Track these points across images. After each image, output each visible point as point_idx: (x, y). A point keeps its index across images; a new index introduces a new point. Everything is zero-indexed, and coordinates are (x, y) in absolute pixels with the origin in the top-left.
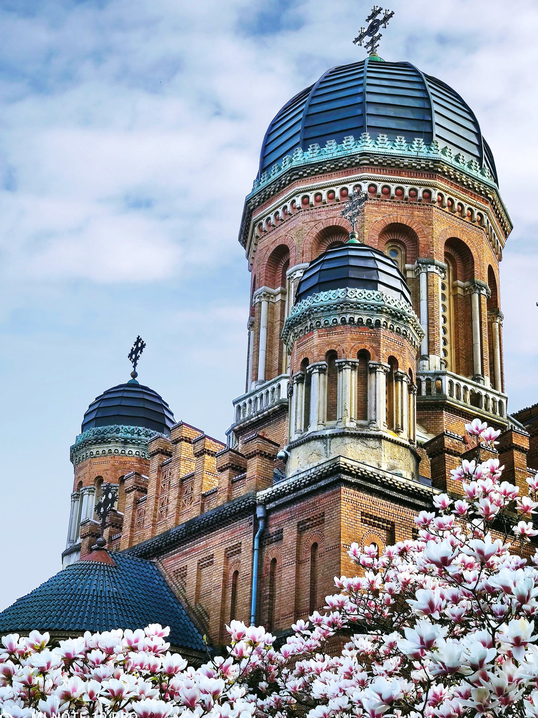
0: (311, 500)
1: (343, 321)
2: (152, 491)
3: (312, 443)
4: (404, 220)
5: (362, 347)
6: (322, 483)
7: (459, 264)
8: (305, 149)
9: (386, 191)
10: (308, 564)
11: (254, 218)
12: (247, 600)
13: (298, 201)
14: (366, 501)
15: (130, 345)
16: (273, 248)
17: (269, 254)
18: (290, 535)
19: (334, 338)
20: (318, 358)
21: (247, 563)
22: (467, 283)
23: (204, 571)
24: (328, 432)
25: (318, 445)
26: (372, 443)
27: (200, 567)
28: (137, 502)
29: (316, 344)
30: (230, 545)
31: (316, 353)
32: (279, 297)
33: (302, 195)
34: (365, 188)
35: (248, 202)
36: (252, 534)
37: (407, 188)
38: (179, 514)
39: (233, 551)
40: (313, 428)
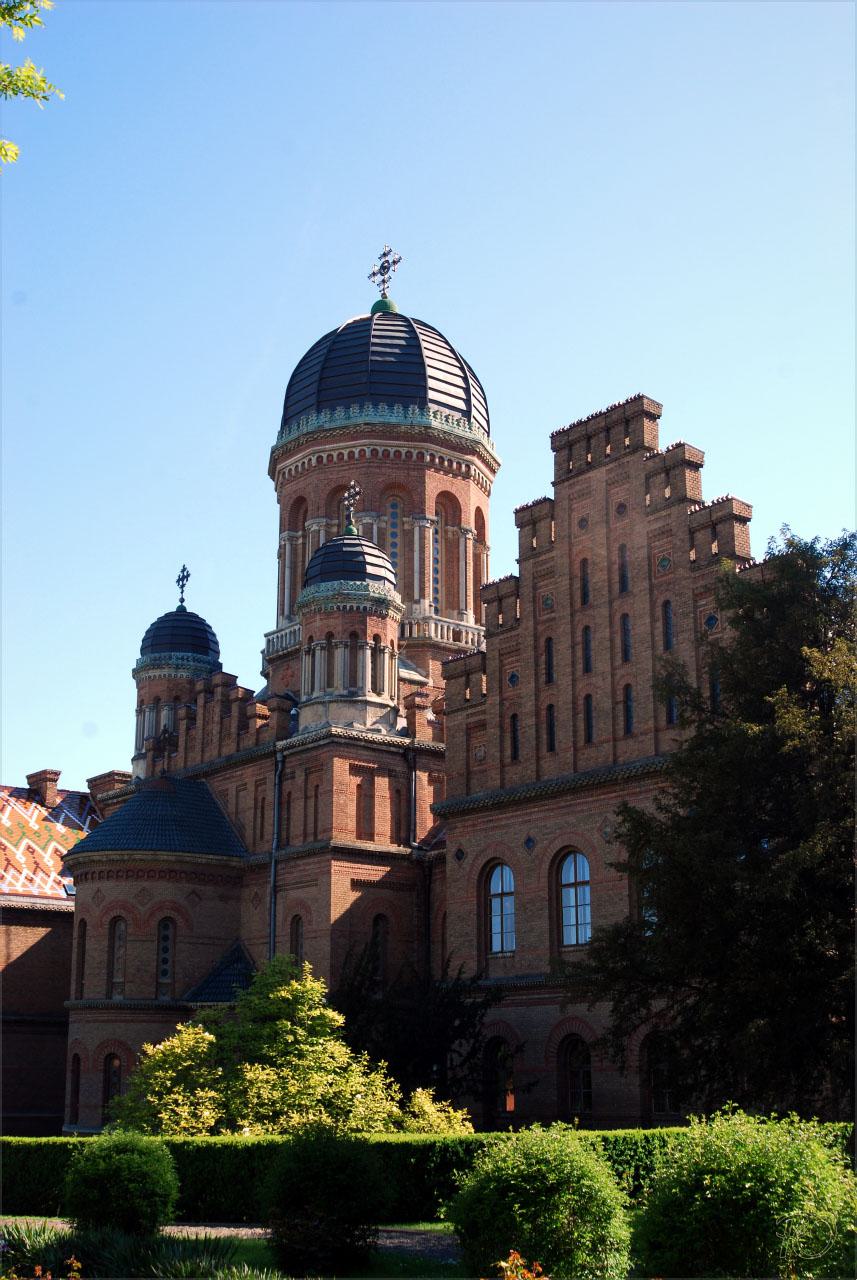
0: (314, 753)
1: (338, 608)
2: (199, 722)
3: (315, 706)
5: (352, 629)
6: (322, 743)
8: (319, 412)
10: (313, 800)
11: (279, 467)
12: (272, 822)
15: (178, 573)
17: (292, 501)
18: (300, 778)
19: (332, 622)
21: (271, 796)
22: (455, 528)
23: (241, 793)
25: (321, 708)
26: (359, 706)
27: (238, 792)
28: (188, 729)
30: (259, 778)
31: (318, 634)
32: (300, 541)
33: (317, 455)
34: (368, 454)
35: (273, 452)
36: (273, 772)
37: (403, 451)
38: (220, 747)
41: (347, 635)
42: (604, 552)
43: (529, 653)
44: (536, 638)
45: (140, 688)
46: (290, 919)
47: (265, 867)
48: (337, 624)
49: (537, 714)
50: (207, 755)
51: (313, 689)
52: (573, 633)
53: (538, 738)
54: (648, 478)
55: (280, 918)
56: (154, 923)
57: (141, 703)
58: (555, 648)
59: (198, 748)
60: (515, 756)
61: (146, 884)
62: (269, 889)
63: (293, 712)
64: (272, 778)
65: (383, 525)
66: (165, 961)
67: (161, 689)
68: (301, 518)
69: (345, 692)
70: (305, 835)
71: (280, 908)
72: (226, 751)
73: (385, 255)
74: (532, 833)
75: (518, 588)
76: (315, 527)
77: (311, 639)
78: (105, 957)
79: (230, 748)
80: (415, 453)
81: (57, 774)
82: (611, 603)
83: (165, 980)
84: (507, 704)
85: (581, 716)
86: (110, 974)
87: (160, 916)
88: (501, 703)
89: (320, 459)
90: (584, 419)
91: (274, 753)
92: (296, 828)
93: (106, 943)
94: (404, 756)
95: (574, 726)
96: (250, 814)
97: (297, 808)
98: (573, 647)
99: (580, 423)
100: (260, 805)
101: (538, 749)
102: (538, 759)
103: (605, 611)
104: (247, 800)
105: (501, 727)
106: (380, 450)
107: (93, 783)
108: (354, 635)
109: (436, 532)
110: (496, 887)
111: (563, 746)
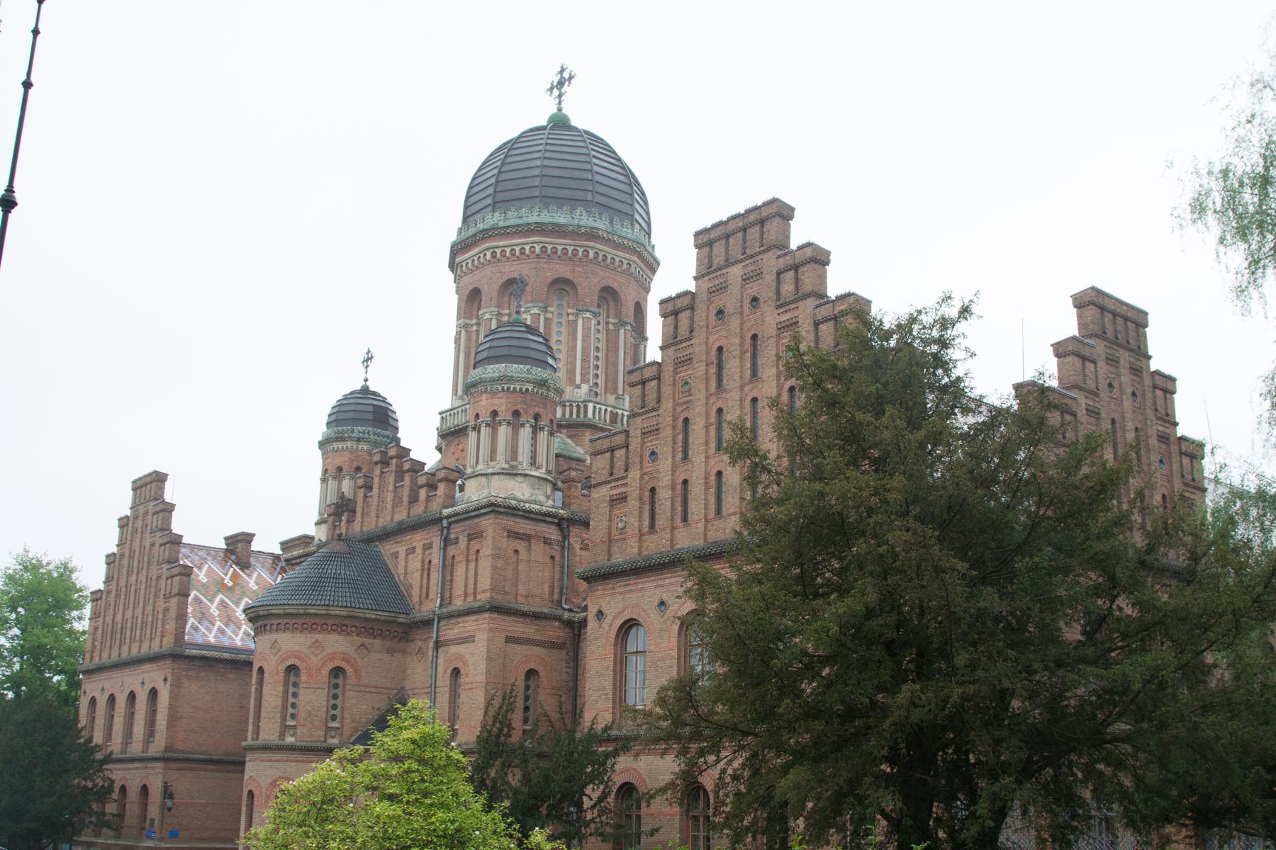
0: (476, 520)
2: (375, 490)
4: (568, 275)
7: (612, 304)
8: (494, 211)
9: (555, 252)
11: (458, 260)
13: (489, 256)
14: (510, 522)
15: (363, 355)
16: (470, 288)
18: (463, 542)
19: (497, 401)
20: (485, 417)
21: (436, 556)
24: (490, 471)
25: (483, 479)
28: (366, 497)
29: (485, 404)
32: (475, 328)
37: (570, 249)
38: (393, 512)
39: (428, 547)
40: (480, 467)
41: (510, 413)
42: (737, 341)
43: (667, 433)
44: (675, 419)
45: (324, 459)
46: (449, 671)
47: (428, 623)
48: (502, 404)
49: (673, 489)
50: (381, 520)
51: (477, 462)
52: (707, 414)
53: (673, 510)
54: (779, 274)
55: (440, 669)
56: (326, 672)
57: (325, 471)
58: (691, 427)
59: (373, 514)
60: (652, 525)
61: (319, 637)
62: (431, 645)
63: (459, 482)
64: (437, 542)
65: (550, 316)
66: (335, 707)
67: (342, 460)
68: (476, 307)
69: (506, 466)
70: (466, 595)
71: (441, 661)
72: (398, 517)
73: (562, 71)
74: (665, 598)
75: (660, 372)
76: (487, 316)
77: (477, 416)
78: (280, 702)
79: (401, 515)
80: (581, 250)
81: (253, 535)
82: (742, 387)
83: (335, 724)
84: (646, 478)
85: (713, 490)
86: (284, 719)
87: (331, 665)
88: (641, 478)
89: (494, 254)
90: (725, 219)
91: (440, 520)
92: (458, 589)
93: (281, 689)
94: (558, 525)
95: (706, 499)
96: (415, 579)
97: (460, 570)
98: (707, 427)
99: (720, 224)
100: (427, 568)
101: (672, 519)
102: (673, 529)
103: (736, 395)
104: (415, 563)
105: (641, 499)
106: (550, 247)
107: (286, 545)
108: (516, 414)
109: (599, 323)
110: (631, 647)
111: (696, 518)
